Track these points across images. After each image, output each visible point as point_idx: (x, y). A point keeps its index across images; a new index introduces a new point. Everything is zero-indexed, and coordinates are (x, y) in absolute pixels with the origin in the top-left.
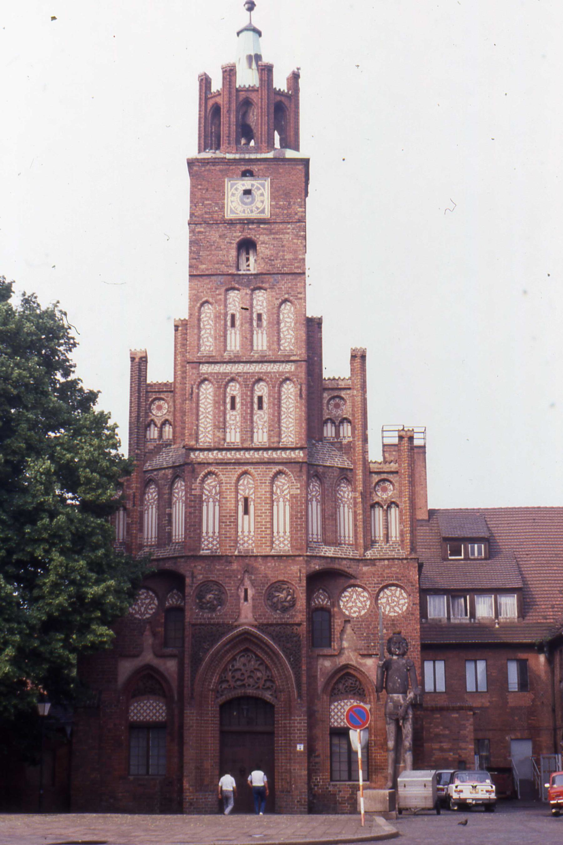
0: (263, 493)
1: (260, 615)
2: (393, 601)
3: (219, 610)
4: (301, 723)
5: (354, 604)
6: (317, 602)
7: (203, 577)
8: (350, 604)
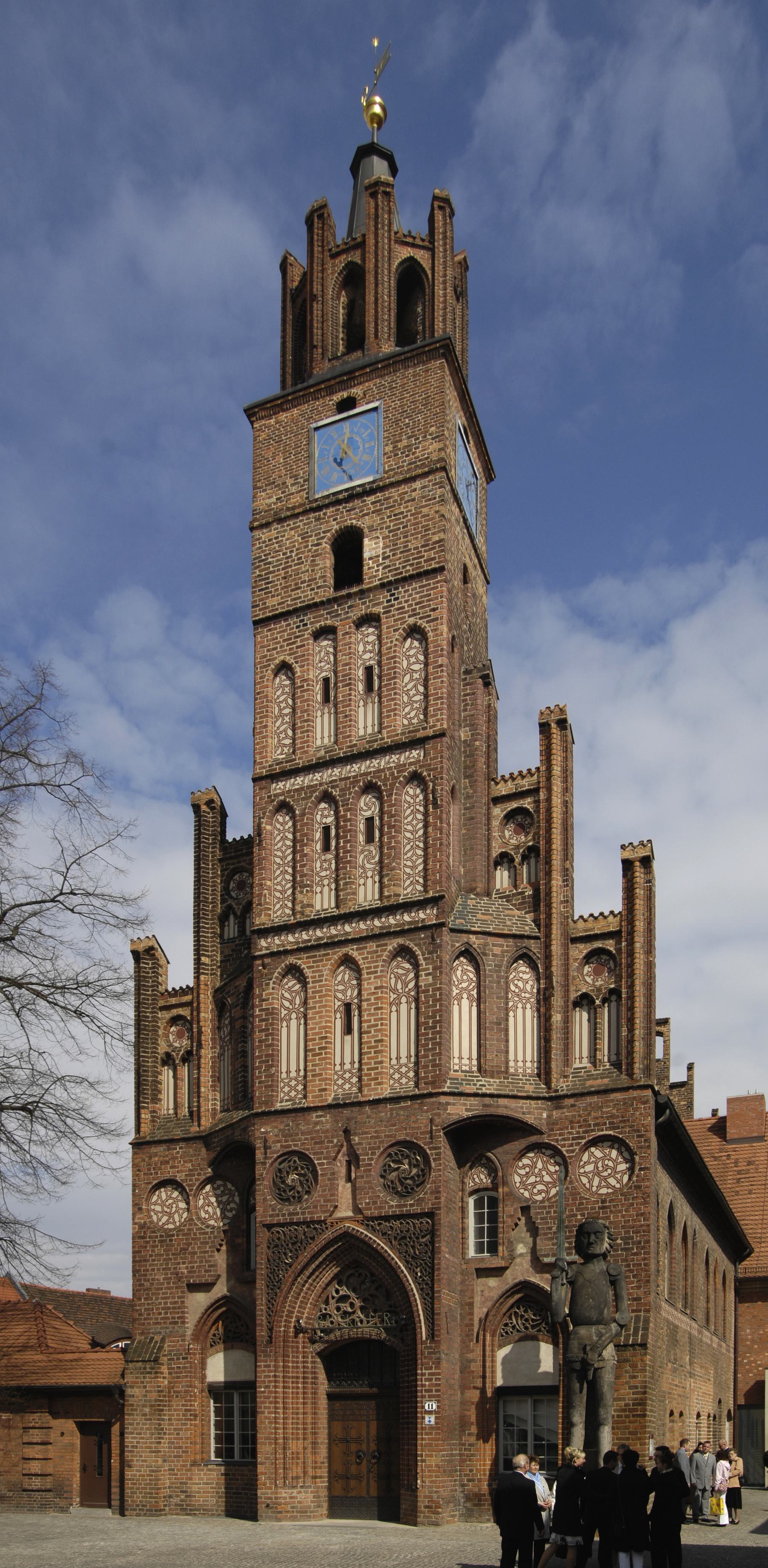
0: (373, 990)
1: (368, 1204)
2: (605, 1169)
3: (306, 1200)
4: (430, 1380)
5: (538, 1179)
6: (477, 1180)
7: (281, 1146)
8: (532, 1179)
